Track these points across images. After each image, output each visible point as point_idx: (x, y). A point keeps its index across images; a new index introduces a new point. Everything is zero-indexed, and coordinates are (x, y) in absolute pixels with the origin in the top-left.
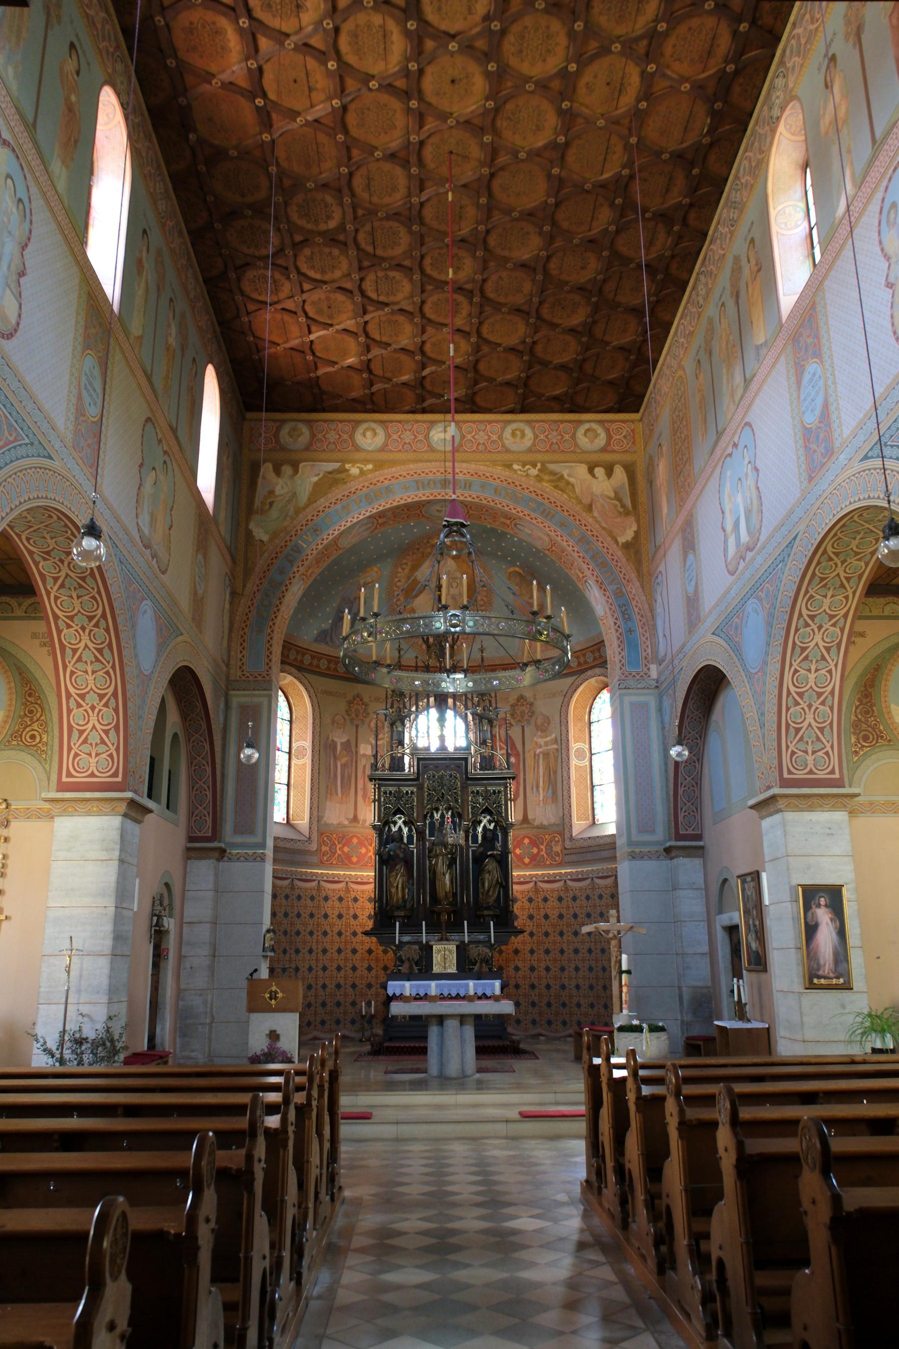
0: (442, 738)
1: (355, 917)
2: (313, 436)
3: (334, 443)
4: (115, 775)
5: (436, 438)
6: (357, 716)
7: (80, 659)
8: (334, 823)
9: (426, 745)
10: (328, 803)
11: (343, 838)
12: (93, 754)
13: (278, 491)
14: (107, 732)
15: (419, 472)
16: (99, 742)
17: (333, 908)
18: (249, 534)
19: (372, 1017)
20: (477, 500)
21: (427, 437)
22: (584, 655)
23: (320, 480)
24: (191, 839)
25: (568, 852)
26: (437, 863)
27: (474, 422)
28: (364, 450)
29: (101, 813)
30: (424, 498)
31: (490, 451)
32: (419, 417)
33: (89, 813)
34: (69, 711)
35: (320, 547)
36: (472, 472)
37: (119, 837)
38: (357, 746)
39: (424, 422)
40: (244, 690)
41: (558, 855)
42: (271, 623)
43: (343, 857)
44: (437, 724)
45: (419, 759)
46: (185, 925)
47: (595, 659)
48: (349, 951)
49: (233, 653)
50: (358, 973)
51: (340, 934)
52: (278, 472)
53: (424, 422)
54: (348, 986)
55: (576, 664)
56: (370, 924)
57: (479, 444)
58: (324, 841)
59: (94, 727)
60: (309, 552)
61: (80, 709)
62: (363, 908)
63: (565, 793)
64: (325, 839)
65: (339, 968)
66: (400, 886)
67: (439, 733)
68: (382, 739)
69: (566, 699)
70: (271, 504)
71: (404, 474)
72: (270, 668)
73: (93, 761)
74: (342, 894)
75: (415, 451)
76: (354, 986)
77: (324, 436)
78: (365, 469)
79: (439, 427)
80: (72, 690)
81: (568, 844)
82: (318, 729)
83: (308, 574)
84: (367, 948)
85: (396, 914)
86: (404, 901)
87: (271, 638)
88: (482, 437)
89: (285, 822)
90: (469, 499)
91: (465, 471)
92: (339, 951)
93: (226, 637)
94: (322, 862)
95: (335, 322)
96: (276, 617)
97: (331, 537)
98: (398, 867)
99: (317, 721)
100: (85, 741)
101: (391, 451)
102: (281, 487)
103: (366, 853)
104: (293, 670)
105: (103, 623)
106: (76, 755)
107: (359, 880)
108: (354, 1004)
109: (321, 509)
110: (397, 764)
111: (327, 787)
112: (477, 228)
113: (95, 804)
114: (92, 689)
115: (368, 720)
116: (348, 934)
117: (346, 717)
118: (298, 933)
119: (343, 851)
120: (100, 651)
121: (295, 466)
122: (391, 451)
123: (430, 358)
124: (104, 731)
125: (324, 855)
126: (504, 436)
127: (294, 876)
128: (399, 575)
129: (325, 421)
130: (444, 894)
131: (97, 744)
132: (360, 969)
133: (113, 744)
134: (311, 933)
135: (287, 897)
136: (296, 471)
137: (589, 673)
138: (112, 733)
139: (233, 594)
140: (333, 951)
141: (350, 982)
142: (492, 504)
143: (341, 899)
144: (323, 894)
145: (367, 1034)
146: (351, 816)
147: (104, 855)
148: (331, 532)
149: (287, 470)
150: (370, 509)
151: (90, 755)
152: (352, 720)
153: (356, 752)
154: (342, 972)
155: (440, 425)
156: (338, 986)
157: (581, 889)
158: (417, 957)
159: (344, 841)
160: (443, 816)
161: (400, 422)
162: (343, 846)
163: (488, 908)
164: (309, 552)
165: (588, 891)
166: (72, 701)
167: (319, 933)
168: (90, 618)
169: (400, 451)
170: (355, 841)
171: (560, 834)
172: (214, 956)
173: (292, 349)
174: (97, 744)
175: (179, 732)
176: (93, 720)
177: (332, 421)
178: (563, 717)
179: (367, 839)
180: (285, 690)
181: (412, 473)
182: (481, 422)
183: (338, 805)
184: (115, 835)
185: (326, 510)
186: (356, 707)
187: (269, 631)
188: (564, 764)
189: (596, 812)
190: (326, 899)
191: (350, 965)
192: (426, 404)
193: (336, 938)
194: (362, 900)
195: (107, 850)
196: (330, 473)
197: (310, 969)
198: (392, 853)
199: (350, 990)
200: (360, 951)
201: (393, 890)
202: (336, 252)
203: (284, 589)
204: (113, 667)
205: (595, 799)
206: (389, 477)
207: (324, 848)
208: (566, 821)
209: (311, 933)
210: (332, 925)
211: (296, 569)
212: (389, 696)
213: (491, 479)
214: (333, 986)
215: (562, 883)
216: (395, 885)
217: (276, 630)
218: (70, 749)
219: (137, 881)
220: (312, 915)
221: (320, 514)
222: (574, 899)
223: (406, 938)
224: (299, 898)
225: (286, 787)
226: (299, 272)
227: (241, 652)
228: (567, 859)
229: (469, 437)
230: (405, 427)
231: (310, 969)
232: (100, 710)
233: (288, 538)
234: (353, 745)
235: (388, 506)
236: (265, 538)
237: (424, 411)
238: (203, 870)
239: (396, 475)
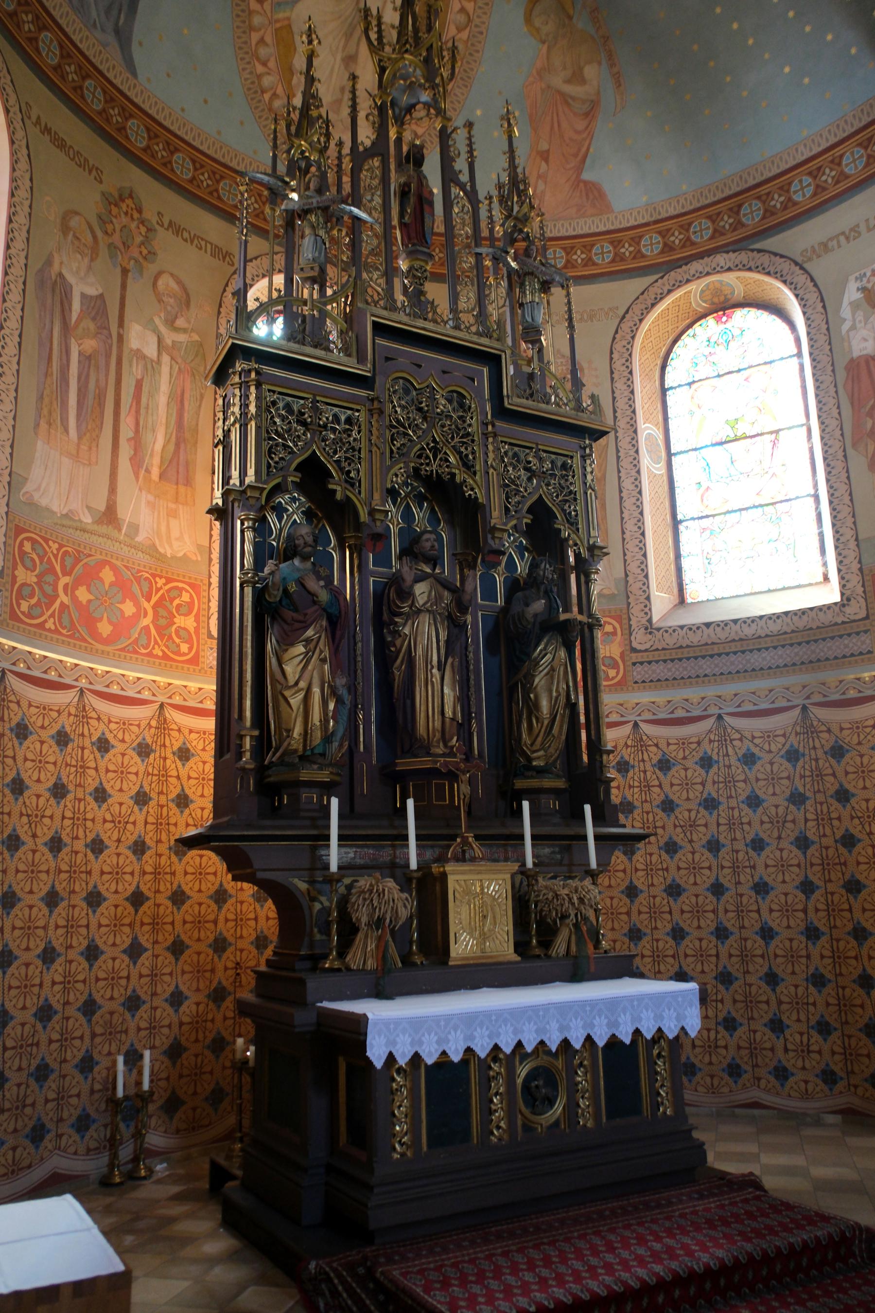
1: (101, 795)
8: (55, 508)
10: (39, 444)
11: (77, 561)
17: (40, 763)
19: (144, 1098)
22: (686, 227)
25: (634, 657)
38: (121, 323)
41: (615, 666)
43: (75, 615)
47: (718, 233)
48: (78, 900)
50: (103, 965)
51: (56, 845)
54: (71, 1011)
55: (658, 248)
58: (22, 554)
62: (122, 773)
63: (630, 526)
64: (27, 547)
65: (48, 956)
66: (316, 690)
68: (185, 331)
69: (626, 326)
74: (67, 723)
76: (89, 1008)
81: (640, 639)
82: (21, 219)
84: (131, 889)
85: (306, 774)
86: (328, 739)
92: (52, 899)
94: (14, 616)
98: (310, 632)
99: (23, 194)
103: (136, 617)
107: (115, 689)
108: (87, 1064)
111: (41, 398)
115: (151, 269)
116: (79, 845)
117: (99, 234)
119: (74, 599)
125: (20, 596)
130: (438, 724)
132: (109, 952)
137: (696, 266)
140: (34, 899)
141: (78, 998)
143: (62, 739)
145: (126, 1152)
146: (102, 507)
152: (111, 246)
153: (121, 338)
154: (58, 966)
156: (45, 1013)
157: (683, 743)
159: (78, 569)
160: (408, 515)
162: (77, 583)
163: (541, 772)
165: (706, 746)
170: (107, 575)
171: (618, 619)
178: (618, 365)
179: (138, 580)
183: (66, 461)
186: (124, 220)
188: (625, 463)
189: (687, 578)
190: (22, 731)
191: (80, 942)
193: (45, 857)
194: (120, 747)
198: (293, 588)
199: (78, 1023)
200: (112, 899)
201: (296, 701)
205: (684, 550)
207: (22, 576)
208: (635, 587)
210: (35, 818)
214: (28, 1016)
215: (627, 729)
216: (302, 684)
222: (664, 765)
228: (639, 673)
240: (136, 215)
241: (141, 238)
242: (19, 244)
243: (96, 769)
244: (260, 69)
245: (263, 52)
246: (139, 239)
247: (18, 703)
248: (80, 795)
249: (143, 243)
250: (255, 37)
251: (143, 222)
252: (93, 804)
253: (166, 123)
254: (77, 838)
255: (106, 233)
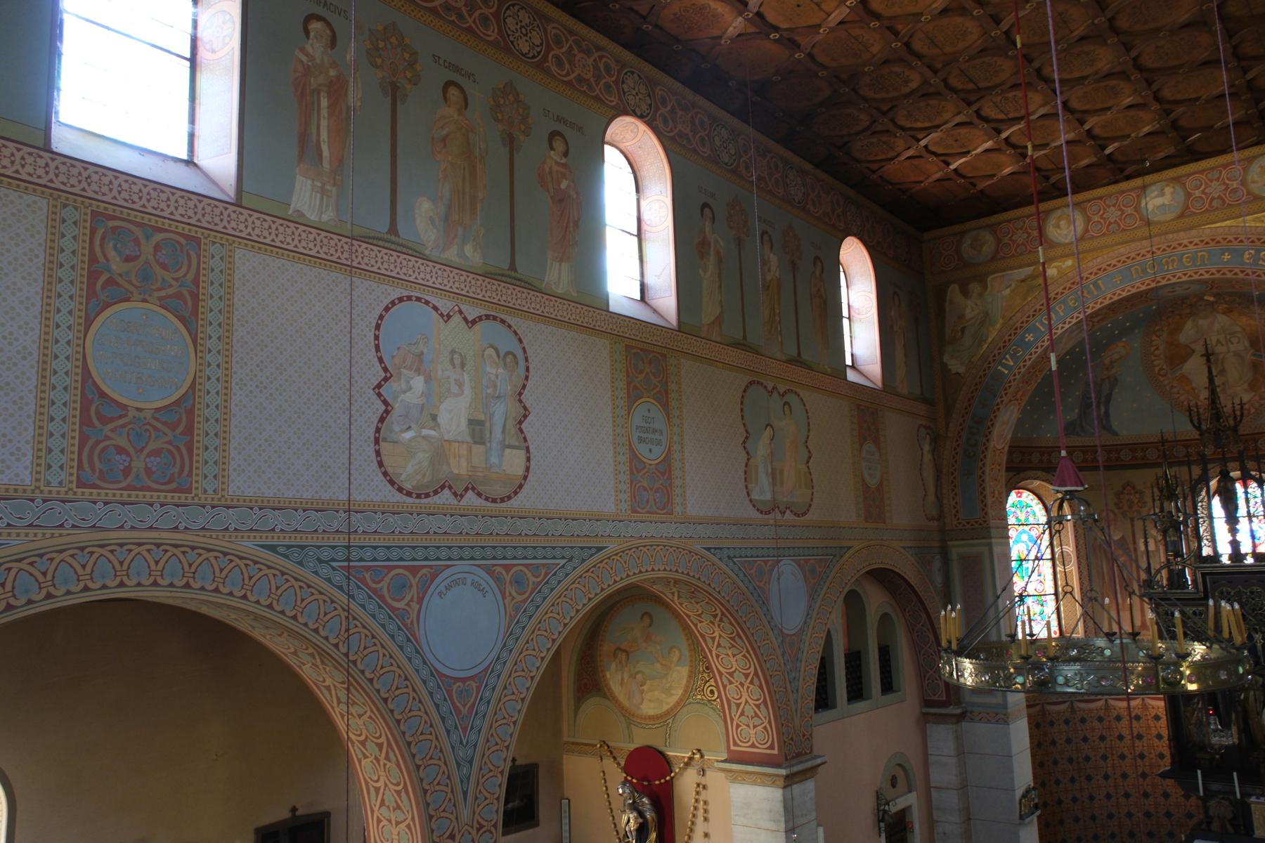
0: (1235, 544)
2: (999, 241)
3: (1023, 244)
4: (772, 747)
5: (1150, 207)
6: (1130, 507)
7: (719, 645)
9: (1211, 553)
12: (751, 726)
13: (969, 313)
14: (758, 706)
15: (1133, 255)
16: (753, 715)
18: (944, 367)
20: (1218, 276)
21: (1137, 209)
23: (1012, 291)
24: (927, 703)
26: (1246, 698)
27: (1201, 172)
28: (1059, 245)
29: (764, 784)
30: (1143, 288)
31: (1229, 205)
32: (1124, 185)
33: (755, 783)
34: (725, 687)
35: (1023, 370)
36: (1207, 240)
37: (782, 810)
39: (1132, 190)
40: (963, 539)
42: (980, 464)
44: (1226, 527)
45: (1204, 575)
46: (932, 789)
49: (945, 501)
52: (965, 293)
53: (1132, 190)
56: (1166, 765)
57: (1213, 199)
59: (747, 702)
60: (1012, 378)
61: (733, 685)
67: (1230, 538)
70: (963, 330)
71: (1114, 262)
72: (986, 514)
73: (752, 732)
75: (1124, 230)
76: (1168, 815)
77: (1011, 239)
78: (1063, 266)
79: (1153, 192)
80: (722, 670)
83: (1018, 396)
87: (983, 481)
88: (1215, 189)
89: (1058, 635)
90: (1207, 276)
91: (1196, 240)
93: (931, 490)
95: (970, 149)
96: (985, 456)
97: (1034, 357)
100: (742, 714)
101: (1093, 237)
102: (971, 309)
104: (1040, 473)
105: (725, 619)
106: (738, 726)
109: (1018, 325)
110: (1176, 579)
112: (1093, 23)
113: (758, 776)
114: (736, 669)
117: (1116, 511)
118: (1087, 759)
120: (733, 639)
121: (982, 281)
122: (1093, 237)
123: (1105, 139)
124: (755, 705)
126: (1249, 178)
127: (1073, 699)
128: (1154, 343)
129: (1009, 221)
131: (752, 718)
133: (765, 718)
134: (1104, 758)
135: (1067, 722)
136: (985, 286)
138: (762, 707)
139: (936, 440)
142: (1241, 276)
144: (1114, 713)
147: (771, 826)
148: (1033, 350)
149: (975, 287)
150: (1076, 315)
151: (748, 726)
155: (1153, 188)
158: (1230, 816)
161: (1100, 198)
164: (1012, 378)
166: (723, 677)
167: (1115, 757)
168: (715, 616)
169: (1104, 234)
172: (969, 819)
173: (938, 180)
174: (752, 718)
175: (889, 610)
176: (745, 696)
177: (1018, 219)
180: (1037, 492)
181: (1123, 258)
182: (1212, 169)
184: (779, 807)
185: (1025, 325)
187: (980, 473)
192: (1127, 173)
195: (774, 821)
196: (1023, 281)
197: (1109, 796)
202: (933, 102)
203: (989, 424)
204: (748, 651)
206: (1095, 270)
209: (1104, 758)
211: (999, 400)
212: (1157, 498)
213: (1235, 243)
217: (987, 469)
218: (732, 720)
219: (821, 830)
220: (1102, 738)
221: (1018, 331)
223: (1215, 787)
224: (1083, 720)
225: (1053, 597)
226: (903, 129)
227: (954, 499)
229: (1197, 193)
230: (1107, 203)
231: (1109, 796)
232: (748, 687)
233: (986, 365)
234: (1130, 540)
235: (1098, 306)
236: (961, 370)
237: (1128, 178)
238: (942, 738)
239: (1104, 266)
240: (1133, 491)
241: (1137, 500)
242: (1082, 541)
243: (1156, 727)
244: (1177, 396)
245: (1175, 390)
246: (1136, 501)
247: (1115, 709)
248: (1149, 737)
249: (1139, 501)
250: (1168, 388)
251: (1136, 492)
252: (1157, 741)
253: (1140, 441)
254: (1151, 753)
255: (1119, 508)
